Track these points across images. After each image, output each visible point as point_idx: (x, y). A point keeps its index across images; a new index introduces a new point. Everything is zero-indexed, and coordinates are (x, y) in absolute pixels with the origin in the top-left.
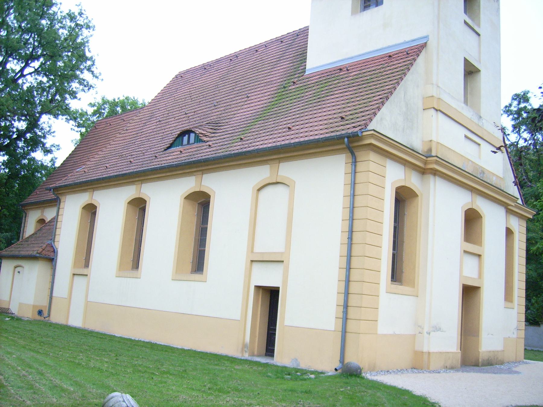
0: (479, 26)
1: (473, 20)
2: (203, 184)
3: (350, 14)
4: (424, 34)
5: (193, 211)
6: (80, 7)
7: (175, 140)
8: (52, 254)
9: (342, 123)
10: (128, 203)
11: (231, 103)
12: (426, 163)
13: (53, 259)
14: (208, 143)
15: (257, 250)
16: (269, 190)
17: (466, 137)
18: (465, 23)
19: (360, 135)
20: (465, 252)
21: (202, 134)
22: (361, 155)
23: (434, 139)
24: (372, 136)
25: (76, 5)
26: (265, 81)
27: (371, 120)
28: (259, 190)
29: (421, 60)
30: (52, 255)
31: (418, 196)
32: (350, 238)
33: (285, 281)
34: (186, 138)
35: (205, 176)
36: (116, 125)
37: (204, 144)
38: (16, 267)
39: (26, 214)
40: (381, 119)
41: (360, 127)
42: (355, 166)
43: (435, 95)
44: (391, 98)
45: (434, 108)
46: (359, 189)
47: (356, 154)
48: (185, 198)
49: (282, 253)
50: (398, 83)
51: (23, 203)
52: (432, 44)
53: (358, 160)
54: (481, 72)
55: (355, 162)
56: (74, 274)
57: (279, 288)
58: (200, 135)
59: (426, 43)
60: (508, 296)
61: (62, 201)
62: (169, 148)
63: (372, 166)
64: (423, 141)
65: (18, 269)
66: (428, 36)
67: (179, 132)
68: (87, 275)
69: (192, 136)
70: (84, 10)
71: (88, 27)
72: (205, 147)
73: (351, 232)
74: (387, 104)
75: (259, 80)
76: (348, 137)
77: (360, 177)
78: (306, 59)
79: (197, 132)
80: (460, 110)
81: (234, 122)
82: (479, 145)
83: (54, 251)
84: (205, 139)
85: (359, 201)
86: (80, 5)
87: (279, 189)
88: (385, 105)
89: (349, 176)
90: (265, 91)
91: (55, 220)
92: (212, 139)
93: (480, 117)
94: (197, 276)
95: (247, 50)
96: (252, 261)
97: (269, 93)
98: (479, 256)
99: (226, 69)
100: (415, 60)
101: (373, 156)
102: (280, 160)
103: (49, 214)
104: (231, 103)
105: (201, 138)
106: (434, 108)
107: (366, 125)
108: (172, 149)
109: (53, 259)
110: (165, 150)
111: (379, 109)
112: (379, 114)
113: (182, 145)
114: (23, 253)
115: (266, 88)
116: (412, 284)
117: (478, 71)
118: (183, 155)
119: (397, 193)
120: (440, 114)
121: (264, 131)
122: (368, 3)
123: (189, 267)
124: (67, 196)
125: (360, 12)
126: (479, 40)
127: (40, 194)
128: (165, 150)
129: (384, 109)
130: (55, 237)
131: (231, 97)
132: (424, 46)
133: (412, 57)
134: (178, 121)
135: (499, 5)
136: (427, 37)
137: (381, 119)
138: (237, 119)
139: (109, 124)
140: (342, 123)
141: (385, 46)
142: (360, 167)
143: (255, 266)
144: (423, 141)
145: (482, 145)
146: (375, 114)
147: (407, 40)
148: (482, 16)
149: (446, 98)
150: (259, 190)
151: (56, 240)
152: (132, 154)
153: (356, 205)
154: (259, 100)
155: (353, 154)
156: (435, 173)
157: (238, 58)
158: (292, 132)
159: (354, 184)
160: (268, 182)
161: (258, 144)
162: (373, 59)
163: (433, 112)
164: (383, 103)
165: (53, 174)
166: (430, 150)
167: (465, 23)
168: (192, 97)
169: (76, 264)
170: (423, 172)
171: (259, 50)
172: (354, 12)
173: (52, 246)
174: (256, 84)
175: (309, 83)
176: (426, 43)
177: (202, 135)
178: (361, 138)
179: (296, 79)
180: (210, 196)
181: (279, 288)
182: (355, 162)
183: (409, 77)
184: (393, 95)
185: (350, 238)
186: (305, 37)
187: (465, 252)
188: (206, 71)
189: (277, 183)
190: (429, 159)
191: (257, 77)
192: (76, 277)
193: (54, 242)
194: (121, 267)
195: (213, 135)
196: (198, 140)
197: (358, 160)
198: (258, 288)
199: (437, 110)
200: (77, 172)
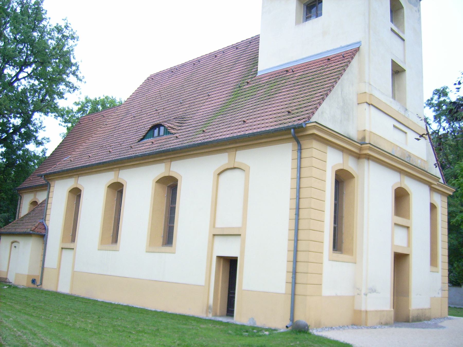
0: (403, 32)
1: (398, 27)
2: (171, 170)
4: (358, 40)
5: (164, 193)
6: (66, 21)
7: (147, 133)
8: (44, 231)
9: (288, 117)
10: (108, 187)
11: (195, 101)
12: (360, 149)
13: (45, 235)
14: (175, 135)
15: (218, 225)
16: (228, 174)
17: (394, 126)
18: (392, 30)
19: (304, 126)
20: (396, 224)
21: (170, 127)
22: (305, 143)
23: (367, 129)
24: (314, 127)
25: (63, 19)
26: (223, 82)
27: (313, 113)
28: (219, 174)
29: (354, 62)
30: (43, 232)
31: (355, 177)
32: (297, 214)
33: (242, 251)
34: (156, 131)
35: (173, 163)
36: (97, 120)
37: (172, 136)
38: (12, 243)
40: (322, 113)
41: (304, 120)
42: (301, 153)
43: (367, 91)
44: (330, 95)
45: (367, 103)
46: (304, 172)
47: (301, 142)
48: (156, 182)
49: (239, 228)
50: (336, 82)
51: (18, 188)
52: (364, 48)
53: (303, 148)
54: (406, 71)
55: (300, 150)
56: (62, 248)
57: (237, 257)
58: (168, 128)
59: (359, 48)
60: (433, 261)
61: (51, 186)
62: (142, 139)
63: (315, 153)
64: (358, 131)
65: (15, 244)
66: (361, 41)
67: (151, 126)
68: (73, 249)
69: (162, 129)
70: (70, 24)
71: (73, 38)
72: (173, 139)
73: (298, 209)
74: (327, 100)
75: (218, 81)
76: (294, 128)
77: (305, 162)
78: (257, 62)
79: (166, 126)
80: (388, 103)
81: (197, 117)
82: (406, 133)
83: (45, 229)
84: (173, 131)
85: (304, 183)
86: (66, 19)
87: (236, 173)
88: (325, 101)
90: (224, 90)
91: (46, 202)
92: (179, 131)
93: (406, 110)
94: (167, 248)
95: (208, 55)
96: (214, 235)
97: (226, 92)
98: (408, 228)
99: (190, 72)
100: (349, 62)
101: (315, 144)
102: (237, 148)
103: (41, 197)
104: (195, 101)
105: (170, 131)
106: (367, 103)
107: (309, 118)
108: (145, 141)
109: (45, 235)
110: (139, 141)
111: (320, 104)
112: (320, 109)
113: (153, 136)
114: (19, 230)
115: (224, 87)
116: (351, 252)
117: (404, 71)
118: (154, 145)
119: (336, 175)
120: (372, 107)
121: (223, 124)
122: (310, 15)
123: (161, 241)
124: (56, 181)
125: (303, 22)
127: (32, 180)
128: (139, 141)
129: (324, 104)
130: (46, 216)
131: (195, 95)
132: (357, 50)
133: (348, 60)
134: (149, 116)
135: (420, 15)
136: (359, 43)
137: (322, 113)
138: (200, 114)
139: (91, 120)
140: (288, 117)
141: (324, 51)
142: (305, 153)
143: (217, 239)
144: (358, 131)
145: (408, 134)
146: (317, 108)
147: (343, 44)
148: (406, 24)
149: (377, 94)
150: (219, 174)
151: (47, 219)
152: (111, 145)
154: (218, 97)
155: (298, 143)
156: (369, 157)
157: (200, 62)
158: (247, 125)
159: (299, 168)
160: (226, 167)
161: (218, 135)
162: (314, 62)
163: (366, 106)
164: (323, 99)
165: (45, 162)
166: (364, 138)
167: (392, 30)
168: (161, 96)
169: (64, 240)
170: (358, 156)
171: (218, 56)
172: (297, 23)
173: (44, 225)
174: (216, 84)
175: (260, 83)
176: (359, 48)
178: (305, 129)
179: (250, 80)
180: (178, 180)
181: (237, 257)
182: (300, 150)
183: (346, 76)
184: (332, 92)
185: (297, 214)
186: (257, 44)
187: (396, 224)
188: (173, 73)
189: (235, 168)
190: (363, 146)
191: (216, 79)
192: (64, 250)
193: (45, 221)
194: (103, 241)
195: (180, 128)
196: (167, 132)
197: (303, 147)
198: (219, 258)
199: (369, 104)
200: (64, 161)
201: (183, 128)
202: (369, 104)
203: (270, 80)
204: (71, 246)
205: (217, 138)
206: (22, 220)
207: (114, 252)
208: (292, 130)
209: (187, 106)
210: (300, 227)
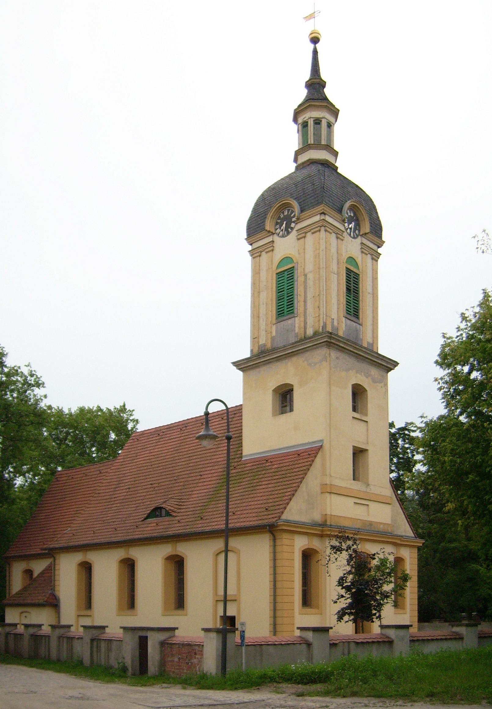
3: (271, 415)
5: (172, 567)
14: (176, 518)
37: (173, 519)
39: (9, 564)
50: (301, 482)
58: (169, 511)
63: (285, 542)
65: (24, 614)
79: (167, 509)
84: (174, 514)
85: (278, 563)
89: (272, 548)
108: (149, 520)
118: (159, 527)
121: (217, 512)
122: (285, 404)
126: (367, 425)
129: (292, 503)
148: (369, 405)
149: (337, 482)
151: (56, 590)
153: (277, 565)
161: (213, 524)
163: (328, 495)
164: (290, 499)
172: (274, 414)
177: (171, 511)
183: (310, 474)
194: (120, 609)
195: (179, 511)
196: (168, 514)
201: (182, 511)
202: (330, 493)
203: (253, 467)
204: (88, 612)
205: (213, 527)
206: (26, 591)
207: (132, 617)
208: (268, 527)
209: (182, 484)
210: (277, 594)
